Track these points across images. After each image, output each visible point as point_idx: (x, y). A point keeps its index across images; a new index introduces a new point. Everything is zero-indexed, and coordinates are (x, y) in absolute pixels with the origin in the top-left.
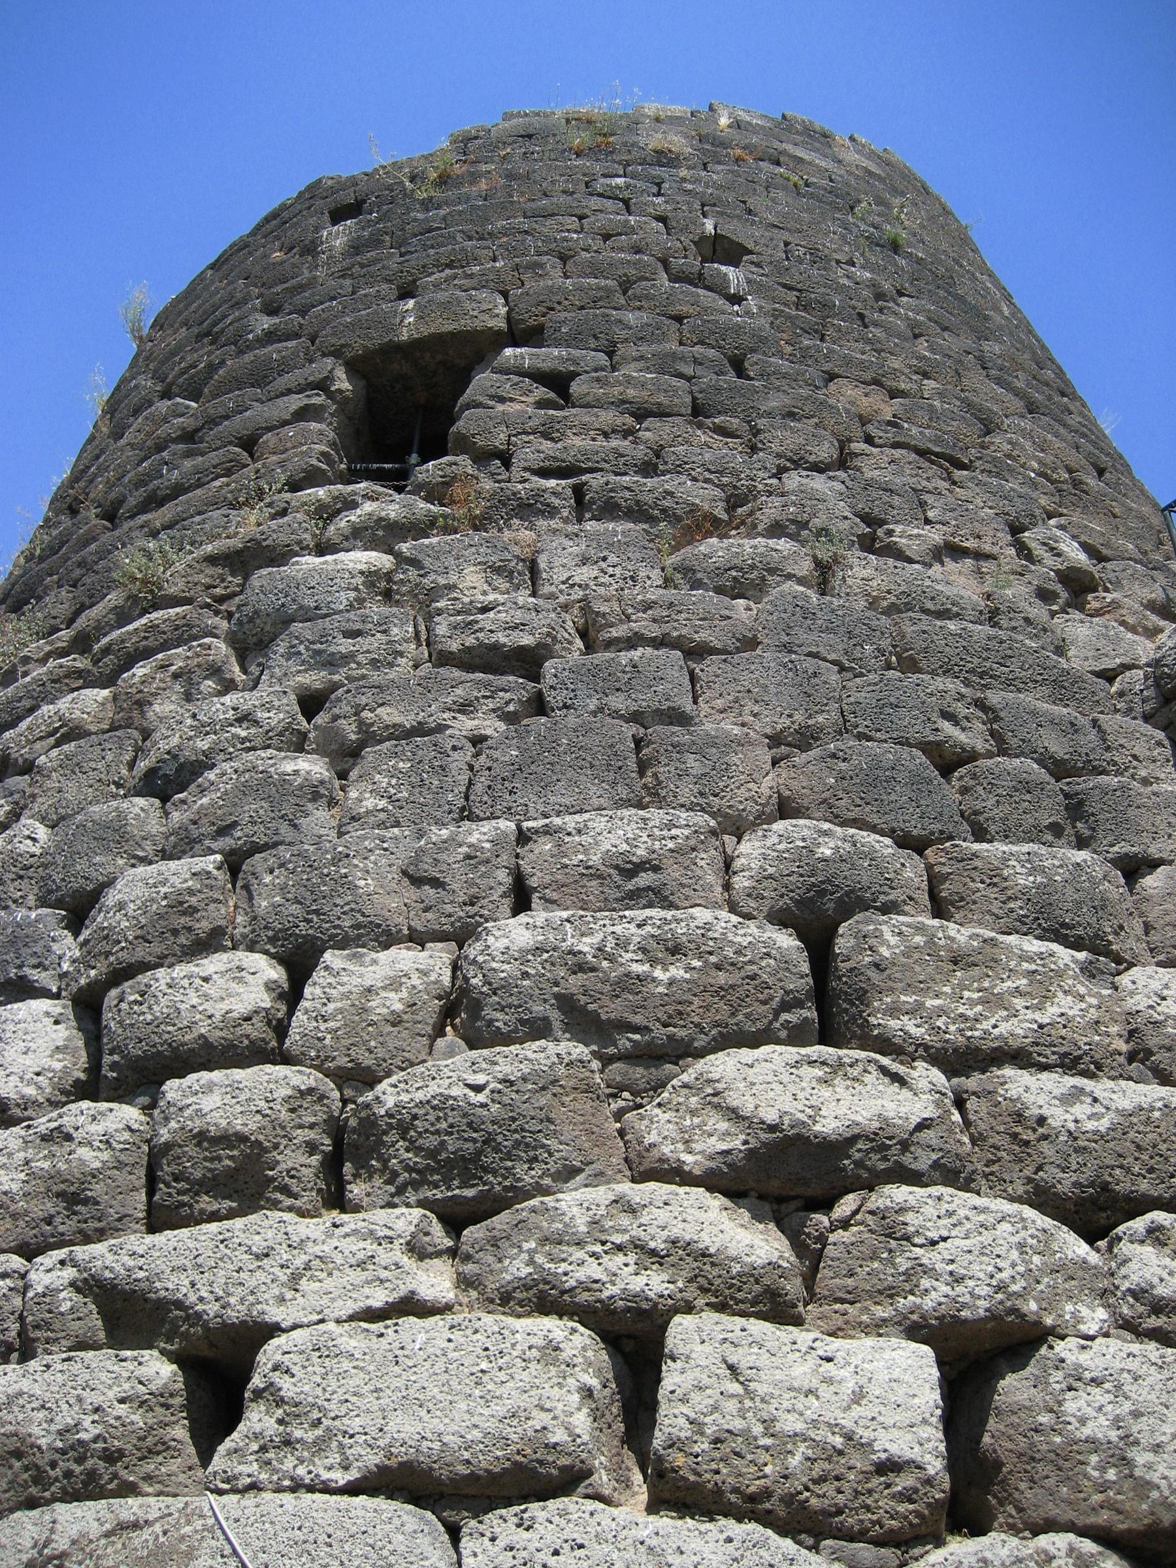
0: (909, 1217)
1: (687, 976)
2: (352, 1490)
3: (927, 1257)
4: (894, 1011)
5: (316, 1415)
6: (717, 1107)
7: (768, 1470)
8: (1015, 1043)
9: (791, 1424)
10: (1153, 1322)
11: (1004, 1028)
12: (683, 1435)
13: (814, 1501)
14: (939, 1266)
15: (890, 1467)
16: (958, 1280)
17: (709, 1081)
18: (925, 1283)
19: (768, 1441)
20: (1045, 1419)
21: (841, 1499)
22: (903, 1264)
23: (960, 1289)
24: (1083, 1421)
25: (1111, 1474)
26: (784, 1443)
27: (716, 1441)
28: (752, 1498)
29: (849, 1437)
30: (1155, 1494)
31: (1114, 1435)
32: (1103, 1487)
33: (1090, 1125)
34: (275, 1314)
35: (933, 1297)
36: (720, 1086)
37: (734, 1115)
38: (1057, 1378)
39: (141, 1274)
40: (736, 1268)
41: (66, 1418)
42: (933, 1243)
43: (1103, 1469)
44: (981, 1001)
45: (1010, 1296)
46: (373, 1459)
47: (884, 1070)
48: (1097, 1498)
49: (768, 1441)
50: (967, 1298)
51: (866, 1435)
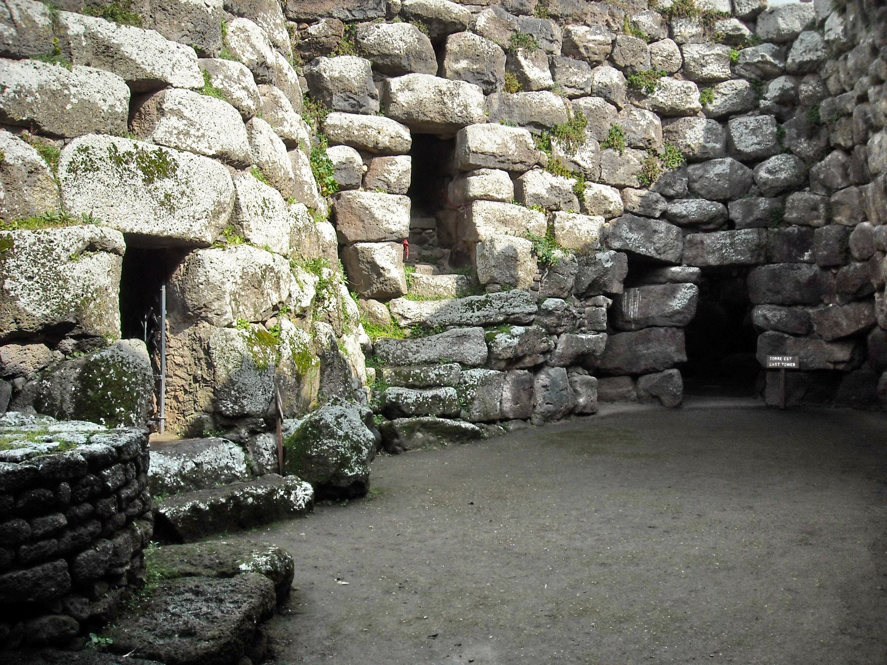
2: (214, 157)
5: (198, 126)
22: (280, 116)
34: (170, 80)
35: (286, 129)
39: (115, 41)
41: (111, 101)
46: (219, 148)
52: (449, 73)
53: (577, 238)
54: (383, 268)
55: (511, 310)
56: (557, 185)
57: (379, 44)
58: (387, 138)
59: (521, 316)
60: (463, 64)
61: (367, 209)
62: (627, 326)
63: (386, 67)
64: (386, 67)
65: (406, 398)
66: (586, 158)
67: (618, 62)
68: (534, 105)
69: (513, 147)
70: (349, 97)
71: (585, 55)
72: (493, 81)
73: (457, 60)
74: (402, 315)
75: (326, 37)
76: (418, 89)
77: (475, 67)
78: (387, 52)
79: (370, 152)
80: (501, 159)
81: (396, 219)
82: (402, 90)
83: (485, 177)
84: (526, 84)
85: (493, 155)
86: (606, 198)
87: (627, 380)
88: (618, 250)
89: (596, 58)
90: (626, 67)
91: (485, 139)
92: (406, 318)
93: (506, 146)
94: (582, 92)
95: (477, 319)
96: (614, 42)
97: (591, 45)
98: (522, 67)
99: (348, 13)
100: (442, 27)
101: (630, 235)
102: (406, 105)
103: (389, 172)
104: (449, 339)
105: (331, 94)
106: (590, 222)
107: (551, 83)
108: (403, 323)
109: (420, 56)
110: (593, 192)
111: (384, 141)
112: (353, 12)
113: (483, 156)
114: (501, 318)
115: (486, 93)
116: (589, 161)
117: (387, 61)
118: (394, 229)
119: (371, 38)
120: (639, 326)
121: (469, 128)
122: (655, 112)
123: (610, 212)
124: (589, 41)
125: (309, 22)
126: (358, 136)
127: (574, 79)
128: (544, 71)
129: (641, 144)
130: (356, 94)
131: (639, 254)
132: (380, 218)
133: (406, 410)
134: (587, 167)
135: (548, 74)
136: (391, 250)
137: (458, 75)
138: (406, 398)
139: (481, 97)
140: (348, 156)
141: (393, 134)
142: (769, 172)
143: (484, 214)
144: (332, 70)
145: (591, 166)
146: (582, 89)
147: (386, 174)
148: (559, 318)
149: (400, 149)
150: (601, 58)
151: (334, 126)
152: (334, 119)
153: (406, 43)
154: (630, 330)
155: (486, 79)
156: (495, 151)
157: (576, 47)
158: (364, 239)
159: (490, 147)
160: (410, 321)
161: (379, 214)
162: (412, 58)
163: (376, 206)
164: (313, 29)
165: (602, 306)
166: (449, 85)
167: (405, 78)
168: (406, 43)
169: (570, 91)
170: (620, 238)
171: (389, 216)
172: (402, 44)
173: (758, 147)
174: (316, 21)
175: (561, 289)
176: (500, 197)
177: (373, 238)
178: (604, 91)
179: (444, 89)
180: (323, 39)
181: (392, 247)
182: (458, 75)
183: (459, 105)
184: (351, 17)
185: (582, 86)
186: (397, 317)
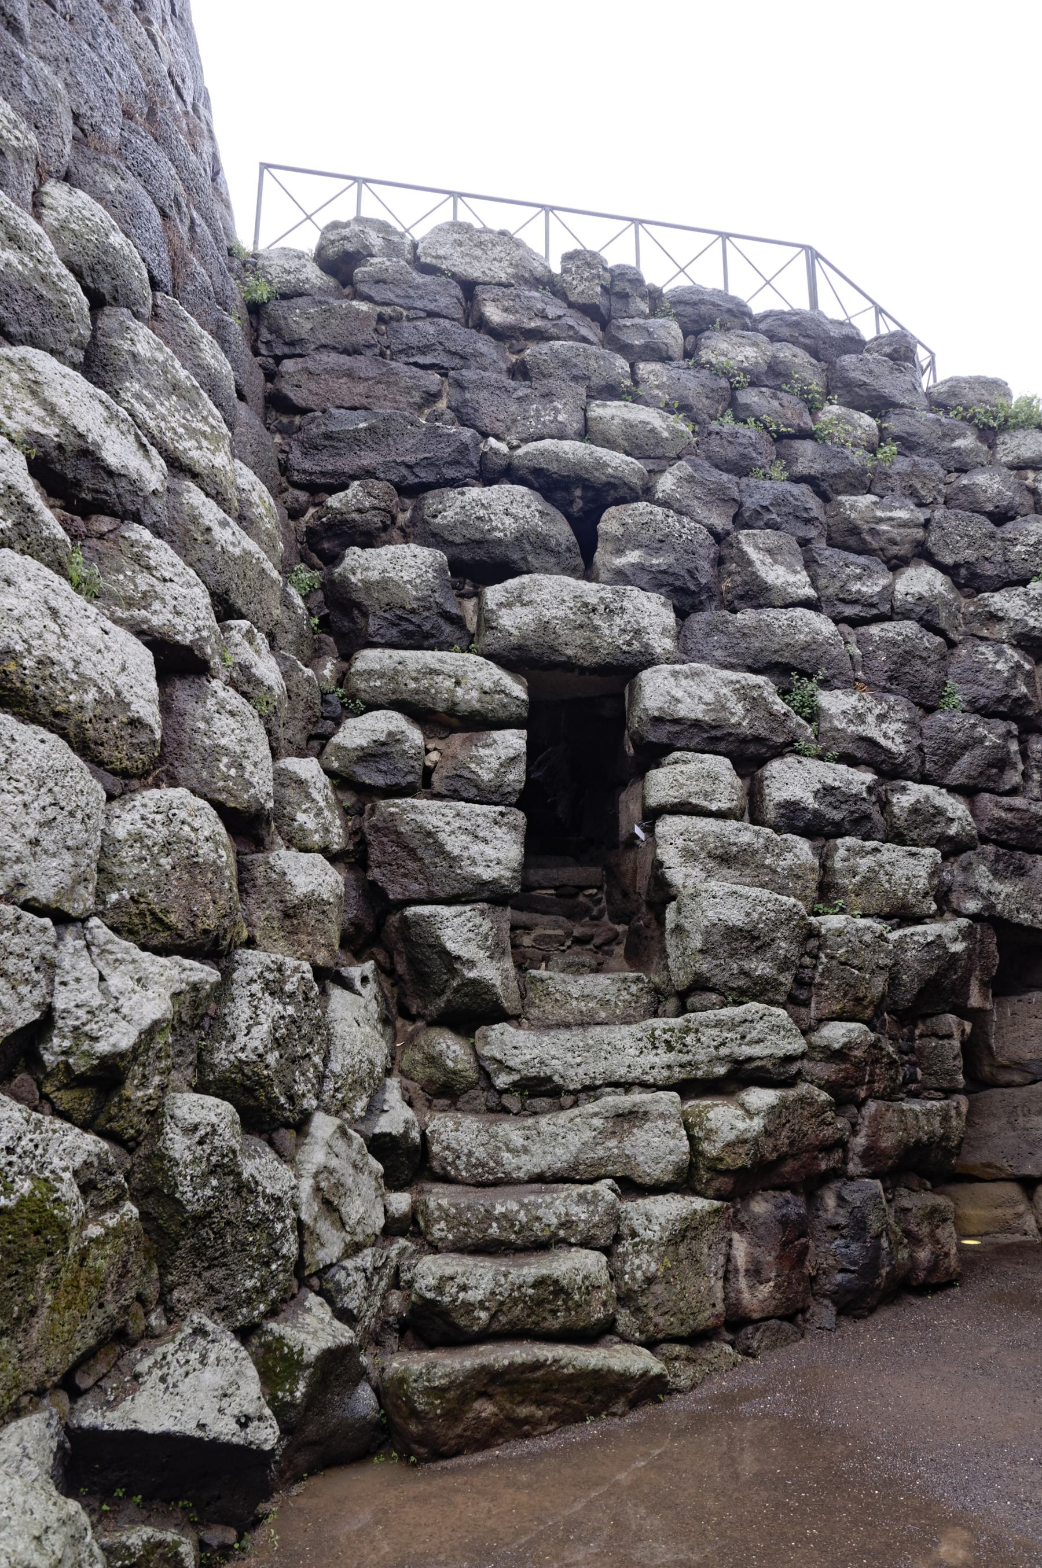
0: (151, 554)
1: (20, 268)
3: (159, 587)
4: (138, 397)
6: (34, 393)
7: (72, 698)
8: (198, 469)
9: (87, 668)
10: (245, 688)
11: (195, 454)
12: (18, 648)
13: (91, 733)
14: (168, 598)
15: (136, 723)
16: (178, 614)
17: (32, 369)
18: (157, 605)
19: (75, 677)
20: (202, 725)
21: (105, 736)
23: (177, 620)
24: (223, 735)
25: (233, 772)
26: (83, 683)
27: (40, 662)
28: (57, 715)
29: (118, 694)
30: (252, 791)
31: (238, 749)
32: (226, 778)
33: (231, 548)
35: (159, 618)
36: (41, 379)
37: (51, 409)
38: (211, 703)
40: (46, 533)
42: (165, 580)
43: (229, 767)
44: (184, 426)
45: (202, 638)
47: (137, 435)
48: (221, 784)
49: (75, 677)
50: (181, 628)
51: (128, 696)
52: (604, 575)
53: (886, 891)
54: (459, 958)
55: (747, 1051)
56: (837, 784)
57: (463, 523)
58: (475, 694)
59: (769, 1066)
60: (633, 556)
61: (429, 834)
62: (1005, 1077)
63: (477, 564)
64: (477, 564)
65: (464, 1288)
66: (891, 734)
67: (938, 558)
68: (779, 631)
69: (739, 709)
70: (400, 618)
71: (875, 545)
72: (693, 588)
73: (620, 552)
74: (500, 1062)
75: (359, 511)
77: (655, 561)
78: (478, 536)
79: (437, 718)
80: (713, 733)
81: (489, 851)
82: (509, 605)
83: (681, 767)
84: (757, 595)
85: (696, 724)
86: (939, 812)
87: (1012, 1190)
88: (974, 917)
89: (894, 550)
90: (957, 566)
91: (679, 694)
92: (510, 1070)
93: (723, 707)
94: (875, 611)
95: (666, 1073)
96: (926, 524)
97: (884, 527)
98: (750, 563)
99: (404, 471)
100: (590, 494)
101: (997, 887)
102: (516, 632)
103: (480, 761)
104: (597, 1122)
105: (365, 615)
106: (913, 861)
107: (810, 592)
108: (502, 1080)
109: (542, 545)
110: (912, 799)
111: (468, 697)
112: (416, 470)
113: (677, 728)
114: (721, 1070)
115: (681, 614)
116: (898, 740)
117: (480, 554)
118: (487, 875)
119: (449, 513)
120: (1030, 1077)
121: (645, 675)
122: (1022, 648)
123: (951, 838)
124: (880, 520)
125: (332, 490)
126: (417, 692)
127: (856, 587)
128: (795, 572)
129: (1002, 708)
130: (413, 611)
131: (1019, 925)
132: (456, 852)
133: (463, 1322)
134: (894, 749)
135: (803, 577)
136: (478, 920)
137: (621, 577)
138: (464, 1288)
139: (669, 618)
140: (392, 728)
141: (488, 685)
143: (680, 842)
144: (367, 569)
145: (903, 749)
146: (873, 605)
147: (473, 766)
148: (859, 1065)
149: (502, 714)
150: (903, 550)
151: (370, 674)
152: (369, 659)
153: (516, 519)
154: (1008, 1085)
155: (678, 583)
156: (700, 716)
157: (854, 530)
158: (424, 896)
159: (690, 709)
160: (516, 1077)
161: (453, 845)
162: (528, 547)
163: (447, 828)
164: (334, 501)
165: (949, 1036)
166: (602, 594)
167: (512, 583)
168: (516, 519)
169: (849, 611)
170: (974, 891)
171: (476, 849)
172: (508, 521)
174: (344, 487)
175: (858, 1000)
176: (714, 807)
177: (442, 894)
178: (917, 609)
179: (593, 600)
180: (354, 515)
181: (482, 913)
182: (621, 577)
183: (623, 631)
184: (412, 480)
185: (875, 599)
186: (491, 1067)
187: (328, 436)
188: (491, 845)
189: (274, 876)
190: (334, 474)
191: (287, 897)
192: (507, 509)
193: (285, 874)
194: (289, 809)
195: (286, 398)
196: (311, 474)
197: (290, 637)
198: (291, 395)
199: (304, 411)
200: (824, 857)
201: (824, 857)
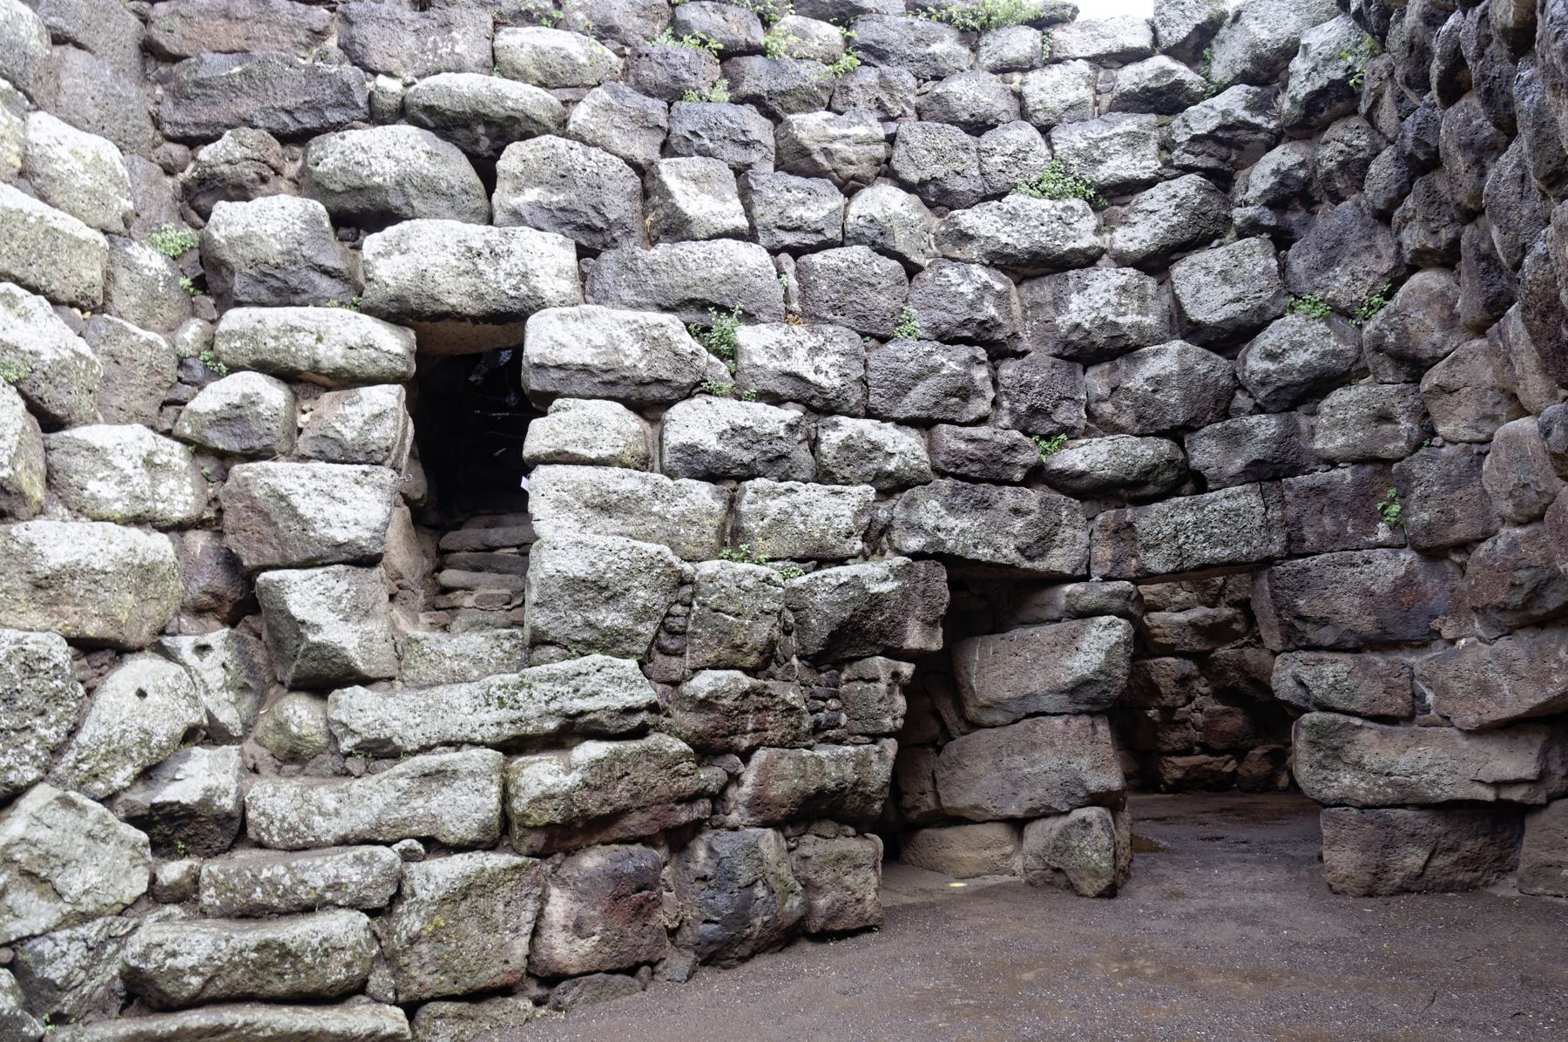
52: (499, 216)
53: (801, 533)
54: (303, 623)
55: (579, 704)
56: (748, 424)
57: (342, 169)
58: (339, 350)
59: (604, 718)
60: (532, 194)
61: (282, 498)
62: (988, 717)
63: (360, 213)
64: (360, 213)
65: (174, 954)
66: (824, 367)
67: (903, 176)
68: (693, 266)
70: (265, 275)
71: (827, 165)
72: (600, 224)
73: (518, 190)
74: (345, 725)
75: (229, 162)
76: (427, 254)
77: (555, 199)
78: (357, 182)
79: (303, 380)
80: (607, 377)
81: (347, 512)
82: (388, 254)
83: (561, 415)
84: (676, 228)
85: (585, 369)
86: (876, 447)
88: (917, 556)
89: (851, 170)
90: (923, 183)
91: (564, 338)
92: (354, 733)
93: (616, 350)
94: (821, 238)
95: (494, 730)
96: (891, 140)
97: (837, 146)
98: (669, 194)
99: (286, 118)
100: (494, 130)
101: (950, 522)
102: (389, 281)
103: (344, 419)
104: (403, 783)
105: (232, 273)
106: (834, 500)
107: (742, 222)
108: (347, 744)
109: (430, 188)
110: (843, 435)
111: (332, 355)
112: (297, 115)
113: (563, 374)
114: (551, 725)
115: (583, 252)
116: (833, 373)
117: (363, 203)
118: (341, 536)
119: (329, 161)
120: (1012, 717)
121: (532, 321)
122: (996, 267)
123: (890, 475)
124: (834, 139)
125: (207, 140)
126: (277, 351)
127: (796, 213)
128: (724, 200)
129: (966, 333)
130: (277, 267)
131: (977, 562)
132: (309, 514)
133: (170, 988)
134: (825, 382)
135: (736, 205)
136: (331, 583)
137: (517, 217)
138: (174, 954)
139: (568, 257)
140: (248, 390)
141: (354, 340)
142: (1271, 356)
143: (552, 494)
144: (230, 224)
145: (837, 382)
146: (819, 232)
147: (338, 425)
148: (728, 714)
149: (372, 370)
150: (865, 169)
151: (231, 335)
152: (235, 319)
153: (398, 161)
154: (993, 726)
155: (580, 221)
156: (588, 360)
157: (804, 152)
158: (278, 561)
159: (576, 354)
160: (358, 740)
161: (306, 508)
162: (412, 191)
163: (301, 491)
164: (205, 153)
165: (876, 680)
166: (488, 237)
167: (391, 231)
168: (398, 161)
169: (790, 239)
170: (915, 528)
171: (331, 510)
172: (389, 165)
173: (1238, 307)
174: (219, 137)
175: (737, 648)
176: (593, 455)
177: (295, 558)
178: (867, 232)
179: (477, 244)
180: (226, 169)
181: (337, 576)
182: (517, 217)
183: (510, 275)
184: (293, 127)
185: (820, 225)
186: (338, 731)
187: (198, 84)
188: (358, 505)
189: (16, 547)
190: (207, 125)
191: (36, 568)
192: (386, 153)
193: (32, 544)
194: (76, 478)
195: (158, 46)
196: (183, 126)
197: (133, 300)
198: (163, 41)
199: (176, 59)
200: (732, 503)
201: (732, 503)
